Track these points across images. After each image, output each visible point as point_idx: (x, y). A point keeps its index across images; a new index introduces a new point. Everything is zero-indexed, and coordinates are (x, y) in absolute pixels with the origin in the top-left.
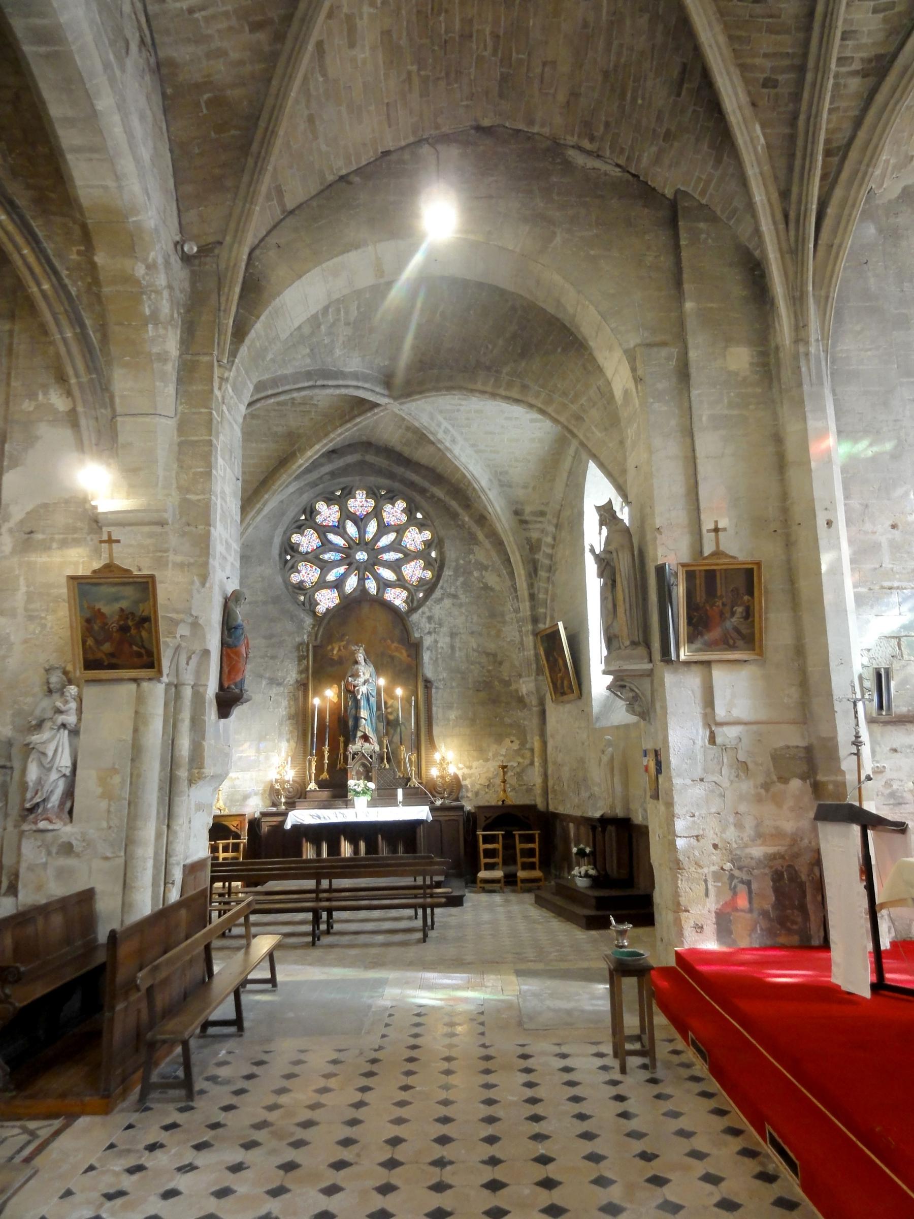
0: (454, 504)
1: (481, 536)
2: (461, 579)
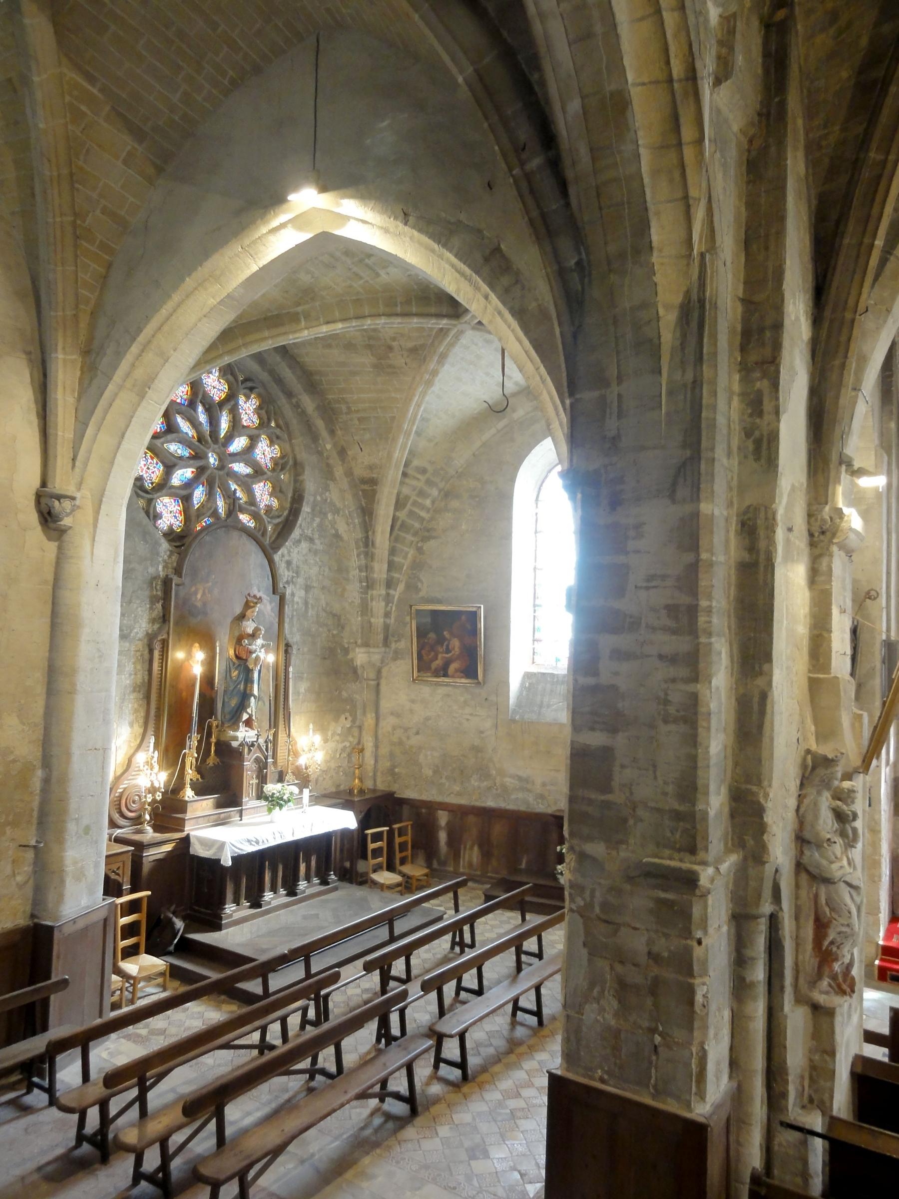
0: (320, 424)
1: (339, 471)
2: (318, 520)
